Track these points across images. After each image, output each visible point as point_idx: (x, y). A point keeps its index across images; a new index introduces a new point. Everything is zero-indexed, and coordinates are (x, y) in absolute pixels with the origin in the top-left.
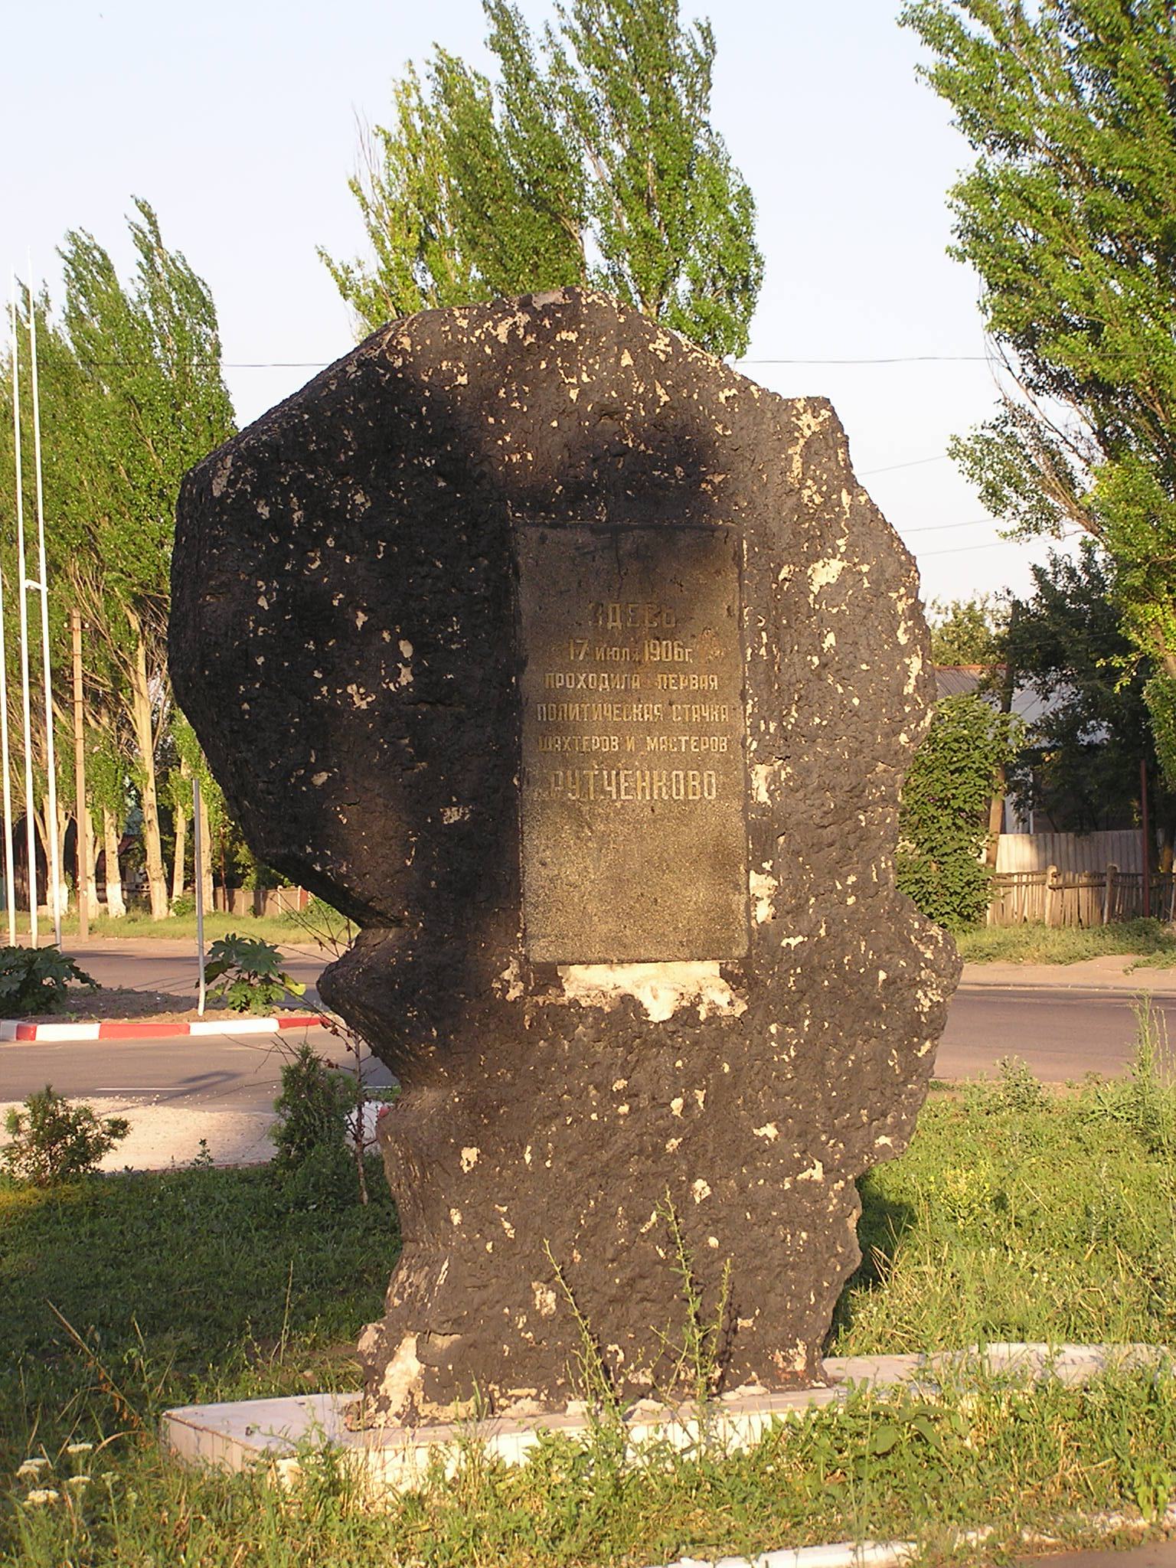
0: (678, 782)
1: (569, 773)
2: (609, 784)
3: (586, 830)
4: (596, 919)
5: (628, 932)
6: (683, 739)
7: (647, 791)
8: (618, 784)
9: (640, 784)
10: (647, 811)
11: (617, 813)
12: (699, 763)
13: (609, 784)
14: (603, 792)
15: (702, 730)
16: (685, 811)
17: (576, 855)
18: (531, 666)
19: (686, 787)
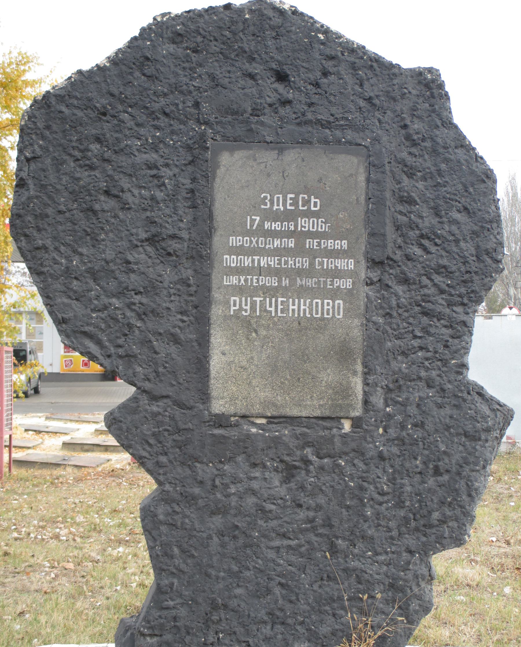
0: (317, 306)
1: (244, 299)
2: (271, 306)
3: (254, 334)
4: (258, 389)
5: (279, 398)
6: (322, 279)
7: (296, 312)
8: (276, 306)
9: (291, 307)
10: (296, 324)
11: (275, 324)
12: (334, 294)
13: (271, 306)
14: (266, 311)
15: (337, 274)
16: (322, 324)
17: (245, 349)
18: (219, 232)
19: (323, 309)
